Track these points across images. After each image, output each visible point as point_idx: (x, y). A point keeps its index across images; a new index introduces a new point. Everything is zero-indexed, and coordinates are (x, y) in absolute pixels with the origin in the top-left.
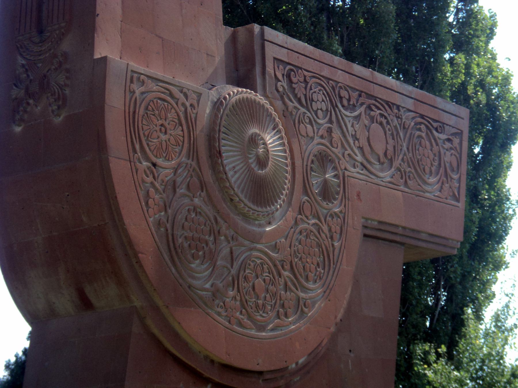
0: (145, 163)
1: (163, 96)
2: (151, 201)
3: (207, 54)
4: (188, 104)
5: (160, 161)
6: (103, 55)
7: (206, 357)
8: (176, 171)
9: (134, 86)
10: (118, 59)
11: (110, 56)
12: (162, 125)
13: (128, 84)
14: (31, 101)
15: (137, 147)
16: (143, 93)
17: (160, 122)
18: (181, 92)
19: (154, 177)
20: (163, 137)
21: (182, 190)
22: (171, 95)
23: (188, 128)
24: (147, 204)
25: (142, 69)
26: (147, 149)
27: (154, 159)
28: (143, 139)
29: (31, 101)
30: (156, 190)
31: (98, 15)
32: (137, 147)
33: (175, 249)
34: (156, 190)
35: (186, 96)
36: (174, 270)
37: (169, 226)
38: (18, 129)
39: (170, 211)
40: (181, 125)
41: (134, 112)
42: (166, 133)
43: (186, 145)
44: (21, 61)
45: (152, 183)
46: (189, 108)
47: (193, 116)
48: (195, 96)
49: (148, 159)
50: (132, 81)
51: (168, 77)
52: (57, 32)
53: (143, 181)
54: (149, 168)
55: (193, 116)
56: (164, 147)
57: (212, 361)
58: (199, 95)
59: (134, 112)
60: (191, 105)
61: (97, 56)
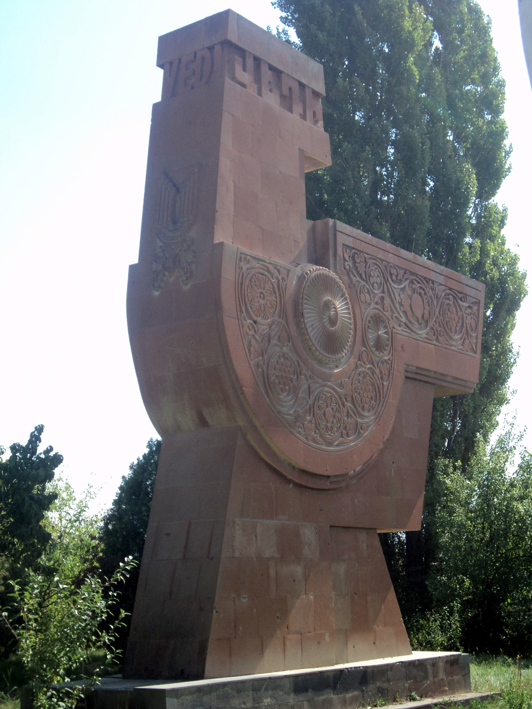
0: (249, 321)
1: (262, 271)
2: (252, 349)
3: (295, 241)
4: (280, 278)
5: (259, 319)
6: (220, 241)
7: (289, 464)
8: (270, 326)
9: (242, 264)
10: (231, 244)
11: (225, 241)
12: (261, 293)
13: (238, 262)
14: (167, 273)
15: (244, 309)
16: (248, 269)
17: (260, 290)
18: (275, 268)
19: (255, 331)
20: (262, 302)
21: (274, 341)
22: (269, 271)
23: (280, 295)
24: (249, 350)
25: (247, 251)
26: (250, 310)
27: (256, 318)
28: (248, 303)
29: (167, 273)
30: (256, 340)
31: (217, 211)
32: (244, 309)
33: (269, 384)
34: (256, 340)
35: (279, 271)
36: (267, 400)
37: (265, 367)
38: (156, 293)
39: (266, 357)
40: (275, 293)
41: (242, 283)
42: (264, 299)
43: (278, 308)
44: (159, 243)
45: (253, 335)
46: (281, 281)
47: (284, 286)
48: (285, 271)
49: (250, 318)
50: (240, 261)
51: (266, 257)
52: (187, 223)
53: (247, 334)
54: (251, 324)
55: (284, 286)
56: (263, 309)
57: (294, 467)
58: (289, 271)
59: (242, 283)
60: (283, 278)
61: (216, 241)
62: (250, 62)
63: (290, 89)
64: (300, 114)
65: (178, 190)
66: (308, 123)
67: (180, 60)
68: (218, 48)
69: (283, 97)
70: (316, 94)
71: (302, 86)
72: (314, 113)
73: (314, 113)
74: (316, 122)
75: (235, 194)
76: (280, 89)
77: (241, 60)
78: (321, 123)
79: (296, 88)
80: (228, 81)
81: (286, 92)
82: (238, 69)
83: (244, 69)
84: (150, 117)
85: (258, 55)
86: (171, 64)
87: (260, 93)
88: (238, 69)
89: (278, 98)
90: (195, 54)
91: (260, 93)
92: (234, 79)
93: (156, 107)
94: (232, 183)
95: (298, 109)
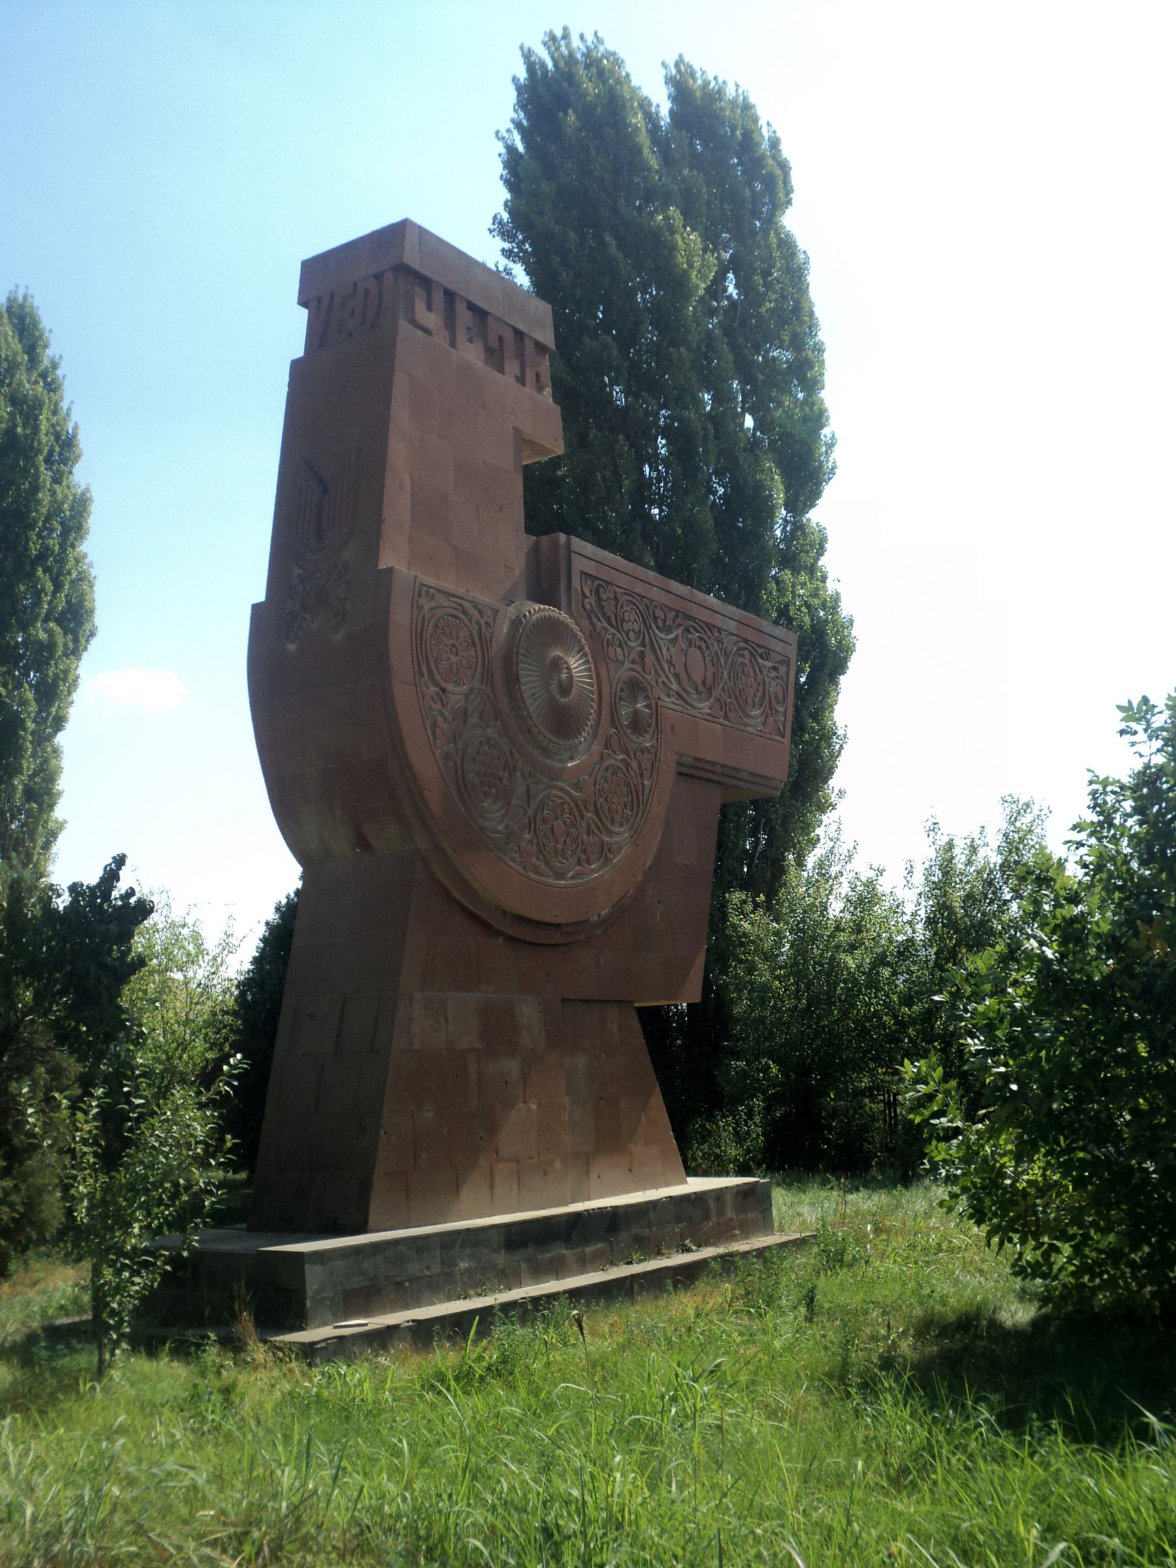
0: (433, 688)
1: (454, 612)
2: (438, 731)
4: (483, 622)
5: (450, 687)
7: (498, 907)
8: (467, 696)
9: (423, 601)
10: (405, 570)
11: (396, 567)
12: (453, 645)
13: (416, 597)
14: (307, 616)
15: (424, 669)
16: (432, 609)
17: (451, 642)
18: (475, 608)
19: (443, 705)
20: (454, 659)
21: (474, 720)
22: (464, 612)
23: (482, 649)
24: (434, 733)
25: (431, 581)
26: (436, 673)
27: (443, 684)
28: (432, 662)
29: (307, 616)
30: (445, 718)
32: (424, 669)
33: (465, 786)
34: (445, 718)
35: (481, 612)
36: (462, 809)
37: (458, 760)
38: (292, 647)
39: (459, 743)
40: (474, 644)
41: (422, 631)
42: (457, 654)
43: (479, 667)
44: (297, 571)
45: (440, 711)
46: (484, 627)
47: (488, 635)
48: (490, 613)
49: (437, 684)
50: (420, 595)
51: (461, 591)
53: (430, 708)
54: (437, 693)
55: (488, 635)
56: (455, 670)
57: (505, 912)
58: (496, 612)
59: (422, 631)
60: (487, 623)
61: (382, 566)
62: (438, 297)
63: (500, 338)
64: (516, 377)
65: (325, 491)
66: (529, 390)
67: (332, 296)
68: (389, 277)
69: (489, 350)
70: (540, 347)
71: (519, 334)
72: (538, 375)
73: (538, 375)
74: (540, 389)
75: (413, 495)
76: (485, 339)
77: (424, 294)
78: (548, 391)
79: (509, 336)
80: (403, 323)
81: (493, 342)
82: (420, 306)
83: (429, 308)
84: (287, 379)
85: (452, 287)
86: (319, 301)
87: (453, 344)
88: (420, 306)
89: (481, 351)
90: (355, 285)
91: (453, 344)
92: (413, 322)
93: (296, 365)
94: (408, 478)
95: (512, 367)
